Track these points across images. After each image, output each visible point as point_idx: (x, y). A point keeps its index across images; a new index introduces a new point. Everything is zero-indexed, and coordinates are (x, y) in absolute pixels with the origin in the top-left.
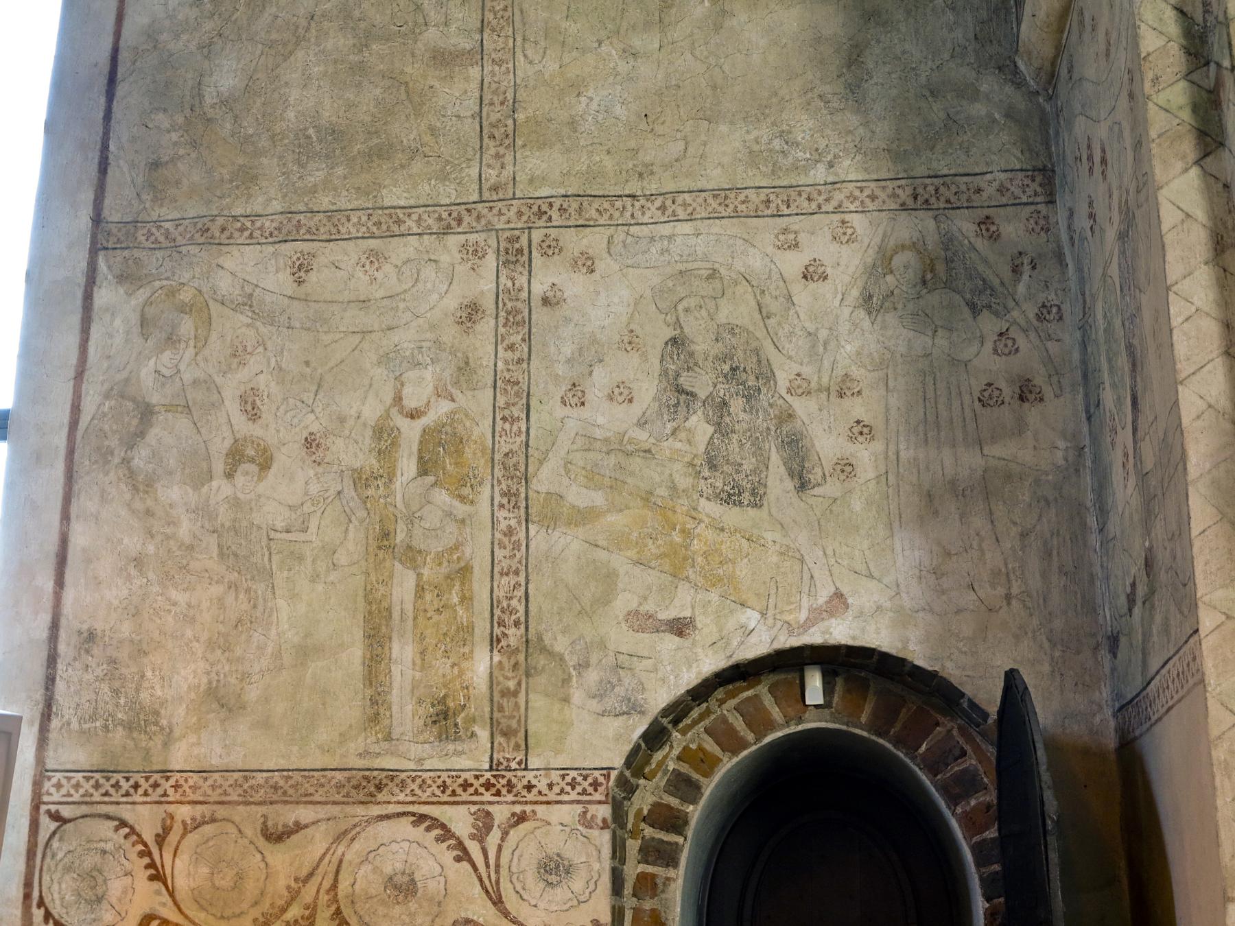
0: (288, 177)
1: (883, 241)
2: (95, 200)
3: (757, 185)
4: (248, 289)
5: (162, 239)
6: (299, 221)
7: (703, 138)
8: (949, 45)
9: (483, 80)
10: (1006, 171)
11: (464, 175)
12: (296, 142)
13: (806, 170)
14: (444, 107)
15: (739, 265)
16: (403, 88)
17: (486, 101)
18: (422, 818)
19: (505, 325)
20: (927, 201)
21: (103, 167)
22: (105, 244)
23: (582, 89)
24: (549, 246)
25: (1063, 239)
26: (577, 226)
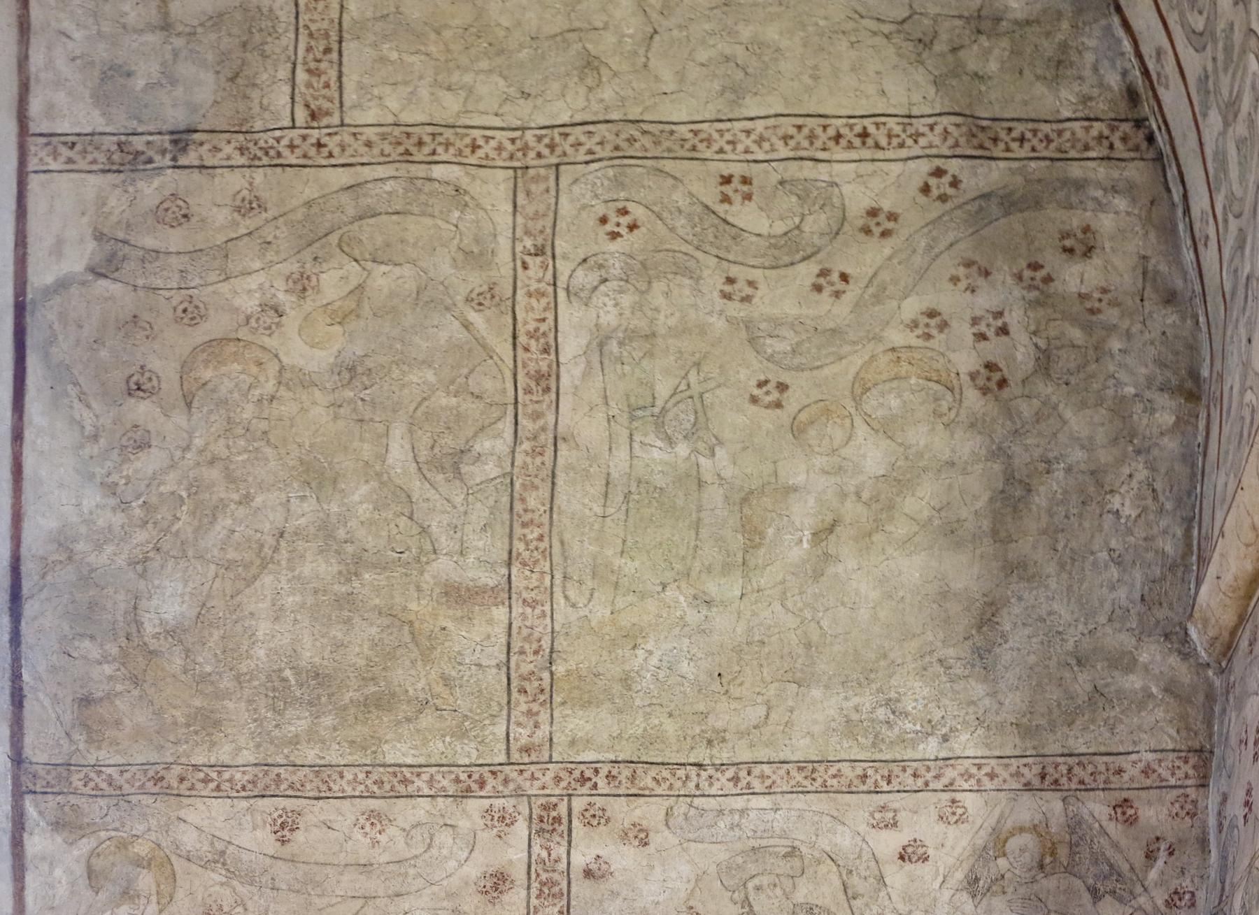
0: (261, 725)
1: (998, 822)
2: (13, 735)
3: (853, 758)
4: (219, 846)
5: (104, 785)
6: (278, 775)
7: (790, 703)
8: (1108, 606)
9: (510, 624)
10: (1155, 751)
11: (487, 733)
12: (269, 684)
13: (914, 744)
14: (459, 653)
15: (824, 843)
16: (406, 628)
17: (515, 648)
19: (538, 897)
20: (1056, 782)
21: (17, 699)
22: (32, 787)
23: (640, 641)
24: (594, 816)
25: (1210, 824)
26: (628, 795)
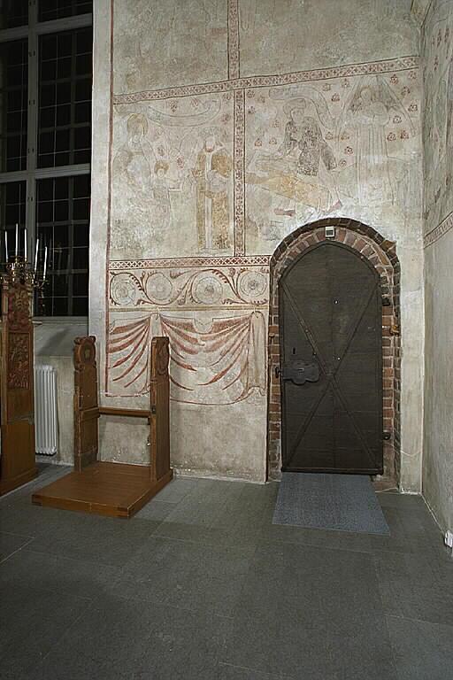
18: (215, 270)
